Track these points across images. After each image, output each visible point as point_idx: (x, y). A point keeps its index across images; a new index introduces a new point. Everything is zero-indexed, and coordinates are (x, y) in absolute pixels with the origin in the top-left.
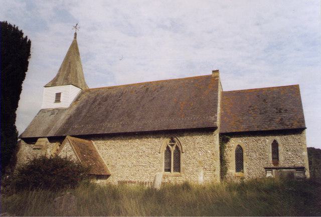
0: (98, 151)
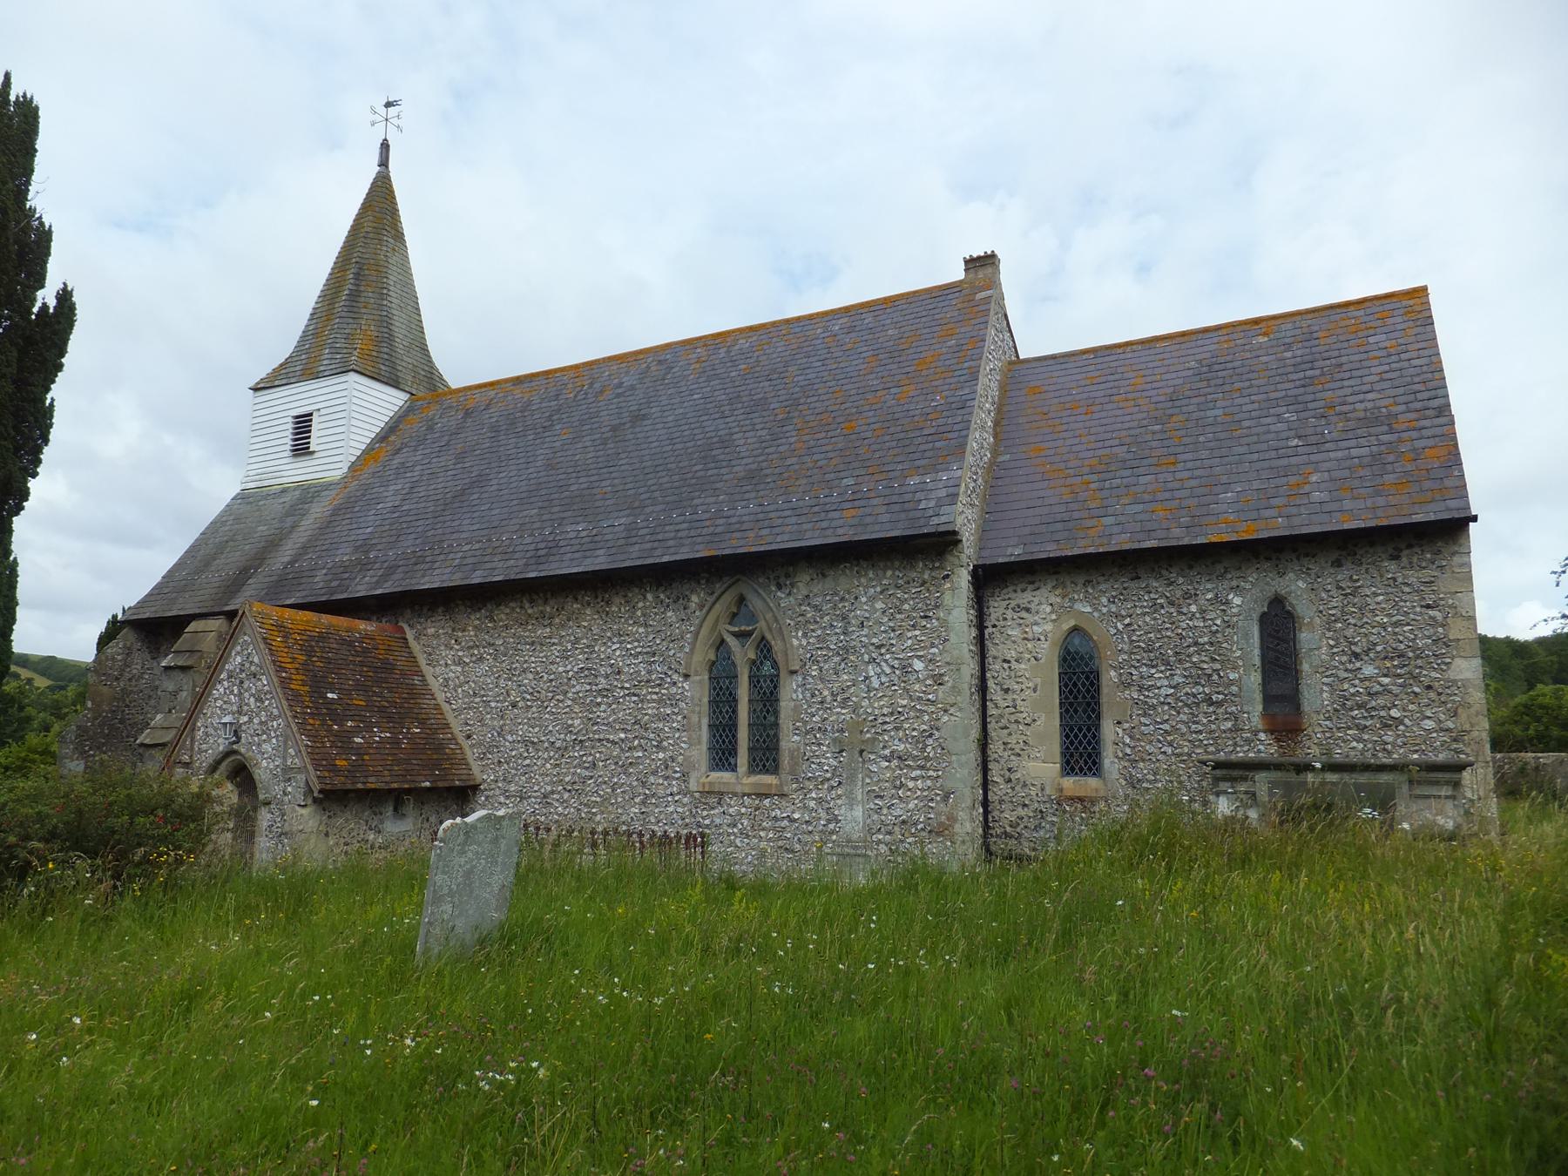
0: (428, 671)
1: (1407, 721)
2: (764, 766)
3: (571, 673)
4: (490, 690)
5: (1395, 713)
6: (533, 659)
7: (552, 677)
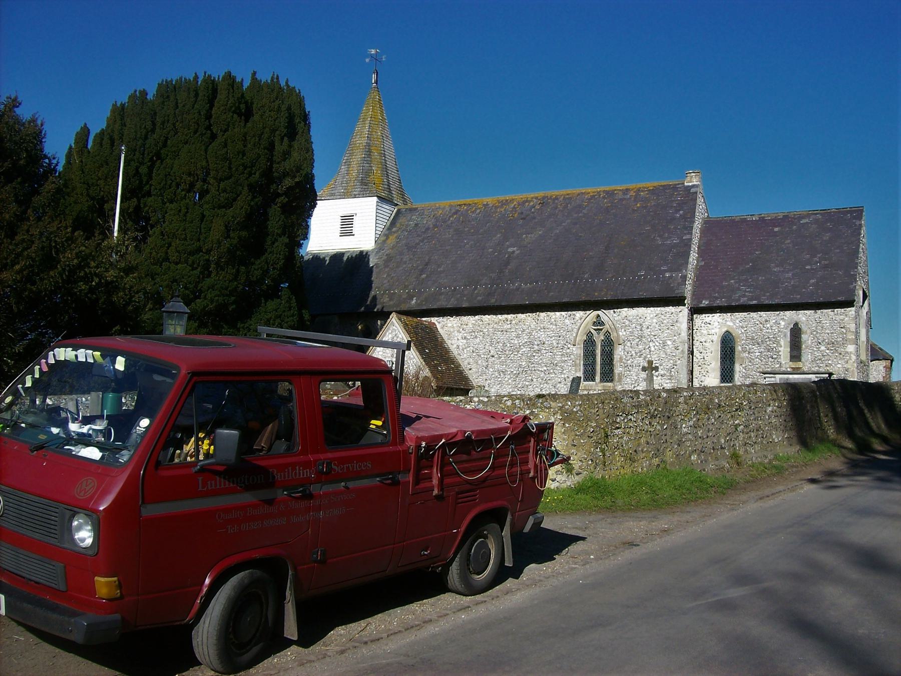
1: (833, 365)
2: (607, 380)
3: (521, 344)
4: (481, 350)
5: (830, 362)
6: (502, 337)
7: (511, 345)
